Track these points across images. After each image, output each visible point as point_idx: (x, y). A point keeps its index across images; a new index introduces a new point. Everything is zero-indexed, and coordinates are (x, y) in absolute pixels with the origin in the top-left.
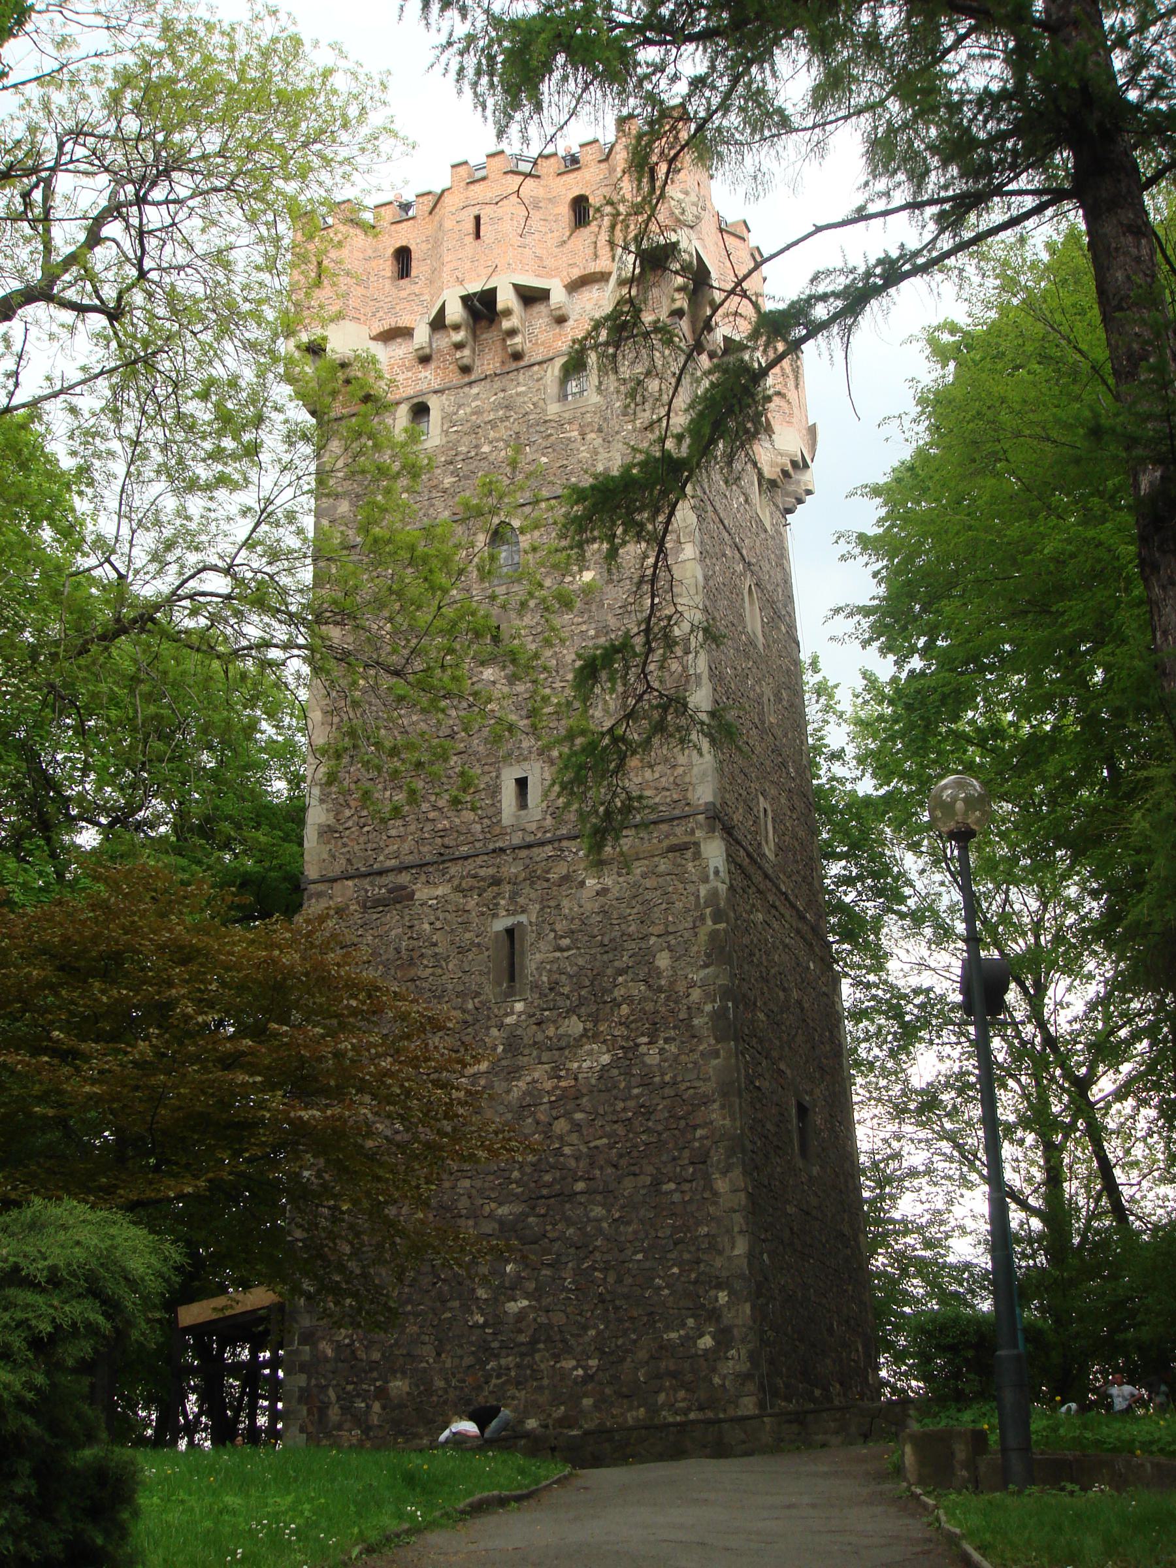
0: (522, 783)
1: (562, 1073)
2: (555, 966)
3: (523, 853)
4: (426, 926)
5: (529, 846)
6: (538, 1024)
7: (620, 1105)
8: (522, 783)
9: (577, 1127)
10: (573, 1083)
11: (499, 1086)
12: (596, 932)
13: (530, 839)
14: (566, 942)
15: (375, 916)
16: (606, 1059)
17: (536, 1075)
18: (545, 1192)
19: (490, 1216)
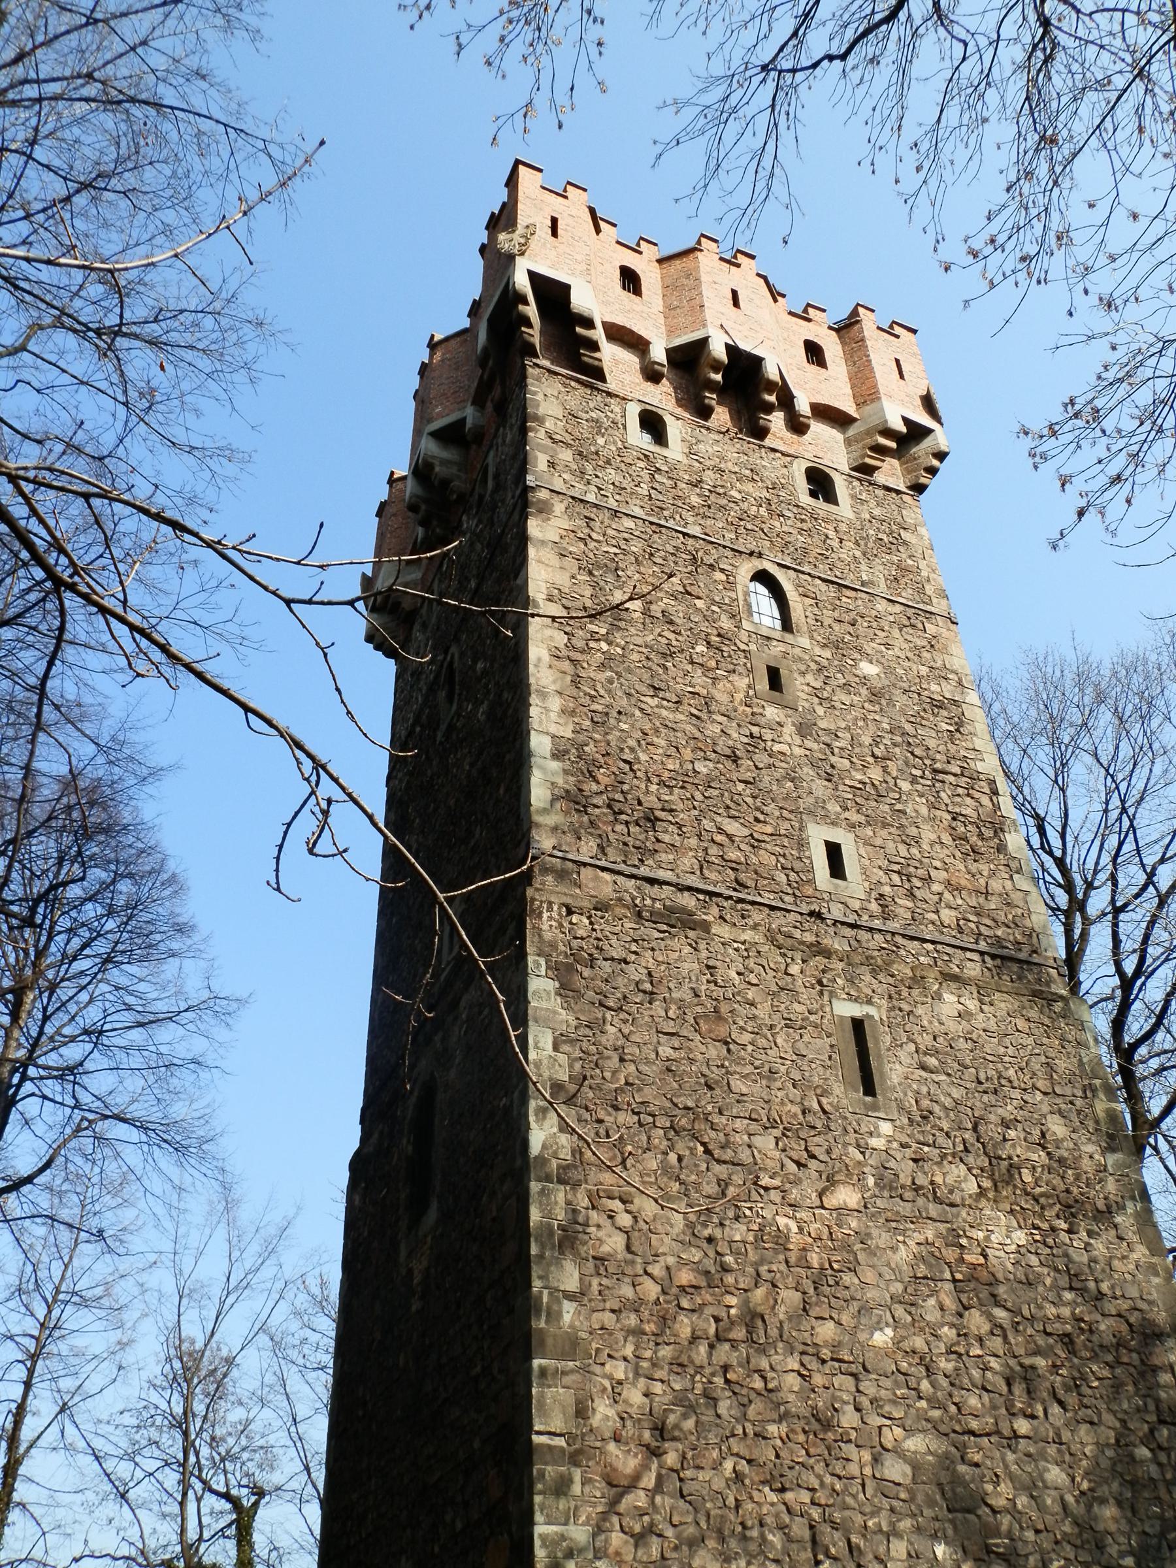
0: (834, 852)
1: (964, 1241)
2: (924, 1090)
3: (848, 932)
4: (733, 974)
5: (853, 926)
6: (915, 1161)
7: (1051, 1311)
8: (834, 852)
9: (997, 1328)
10: (982, 1261)
11: (881, 1238)
12: (968, 1062)
13: (851, 918)
14: (932, 1061)
15: (657, 935)
16: (1020, 1237)
17: (930, 1235)
18: (974, 1424)
19: (897, 1451)
